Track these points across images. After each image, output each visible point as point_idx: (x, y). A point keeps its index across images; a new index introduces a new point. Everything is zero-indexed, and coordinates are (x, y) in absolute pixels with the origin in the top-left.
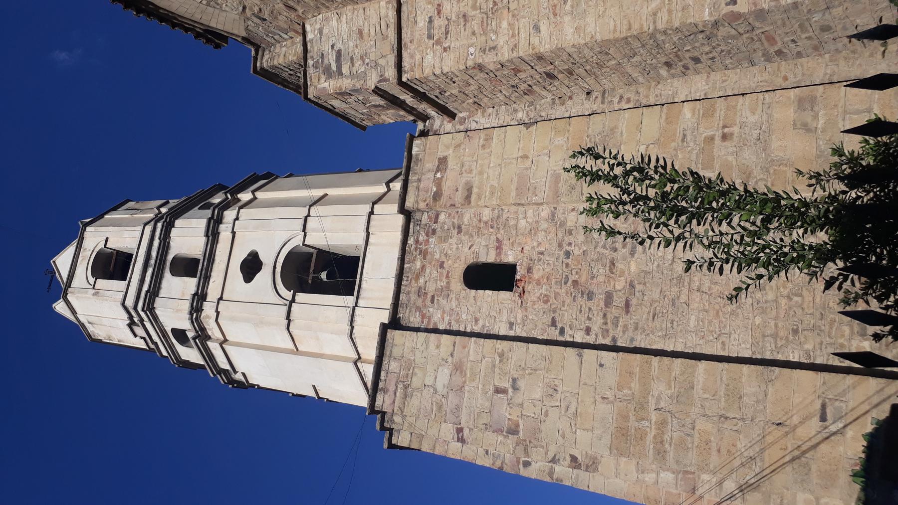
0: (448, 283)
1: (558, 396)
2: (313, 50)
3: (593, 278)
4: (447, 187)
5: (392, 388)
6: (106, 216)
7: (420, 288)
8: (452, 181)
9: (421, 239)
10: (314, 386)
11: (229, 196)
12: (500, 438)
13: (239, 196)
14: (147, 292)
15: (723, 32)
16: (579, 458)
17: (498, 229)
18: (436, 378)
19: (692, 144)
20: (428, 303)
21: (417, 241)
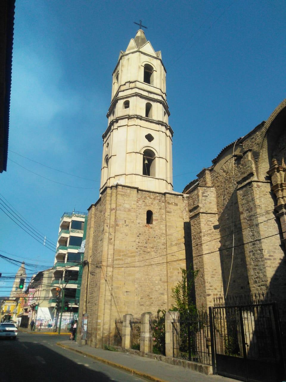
0: (148, 206)
1: (126, 236)
2: (208, 189)
3: (150, 243)
4: (170, 206)
5: (123, 191)
6: (163, 66)
7: (146, 197)
8: (172, 207)
9: (158, 197)
10: (116, 155)
11: (169, 127)
12: (114, 220)
13: (168, 130)
14: (142, 95)
15: (202, 279)
16: (112, 240)
17: (160, 220)
18: (127, 204)
19: (177, 266)
20: (143, 200)
21: (157, 197)
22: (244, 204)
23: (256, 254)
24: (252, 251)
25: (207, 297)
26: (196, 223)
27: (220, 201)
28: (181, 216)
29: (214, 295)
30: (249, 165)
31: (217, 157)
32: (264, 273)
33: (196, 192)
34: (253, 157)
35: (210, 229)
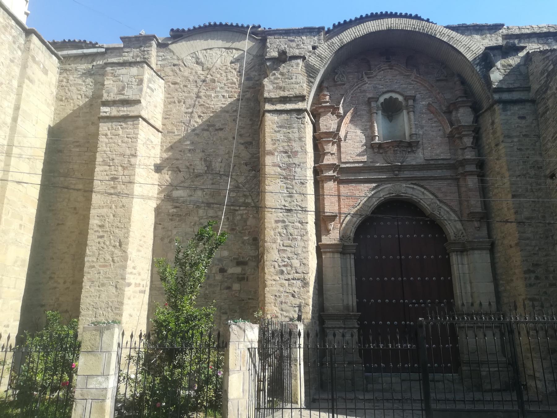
4: (35, 66)
17: (7, 87)
21: (12, 27)
22: (278, 140)
23: (290, 228)
24: (284, 222)
25: (127, 289)
26: (120, 132)
27: (174, 111)
28: (48, 100)
29: (136, 284)
30: (298, 81)
31: (189, 30)
32: (304, 260)
33: (134, 70)
34: (305, 71)
35: (149, 156)
